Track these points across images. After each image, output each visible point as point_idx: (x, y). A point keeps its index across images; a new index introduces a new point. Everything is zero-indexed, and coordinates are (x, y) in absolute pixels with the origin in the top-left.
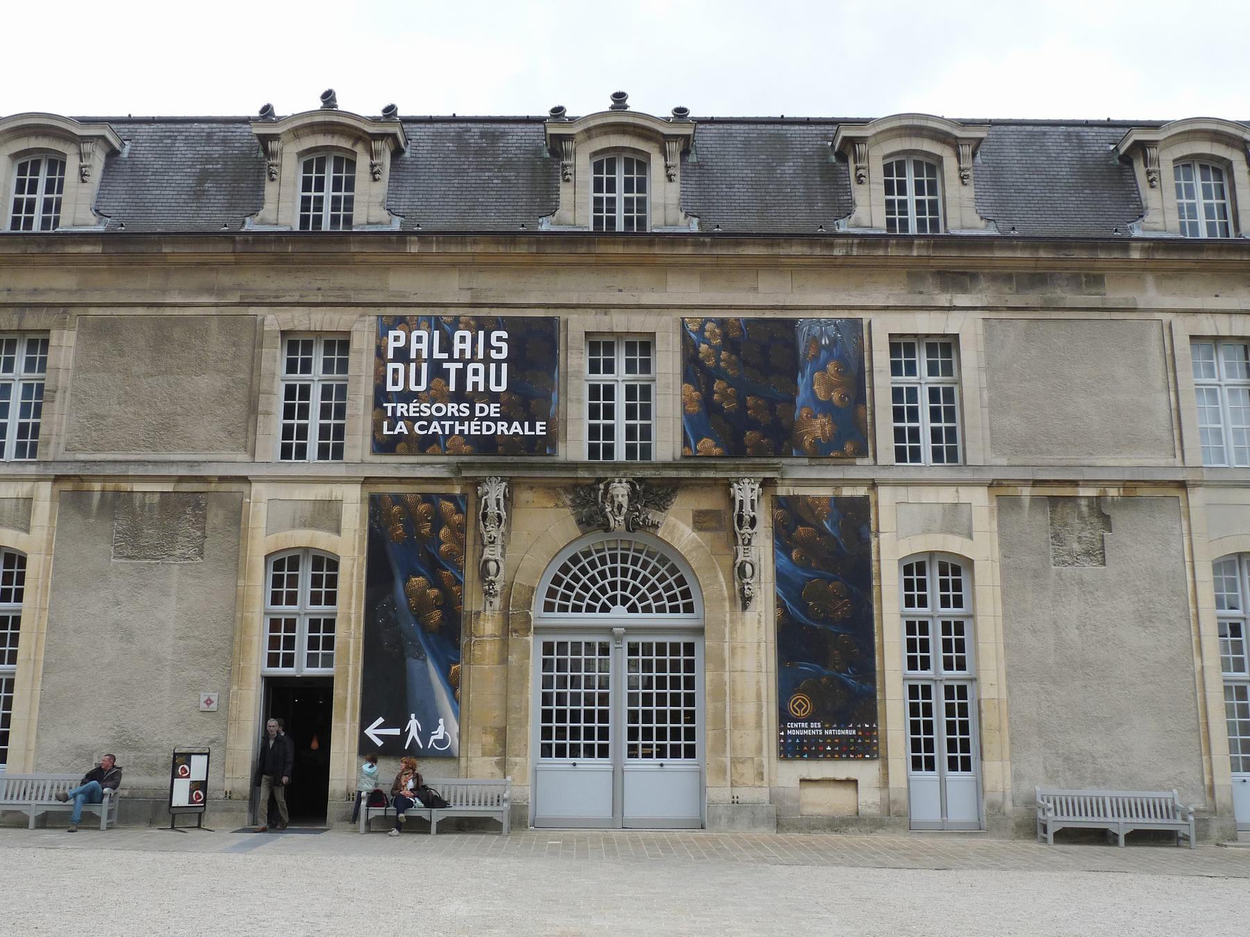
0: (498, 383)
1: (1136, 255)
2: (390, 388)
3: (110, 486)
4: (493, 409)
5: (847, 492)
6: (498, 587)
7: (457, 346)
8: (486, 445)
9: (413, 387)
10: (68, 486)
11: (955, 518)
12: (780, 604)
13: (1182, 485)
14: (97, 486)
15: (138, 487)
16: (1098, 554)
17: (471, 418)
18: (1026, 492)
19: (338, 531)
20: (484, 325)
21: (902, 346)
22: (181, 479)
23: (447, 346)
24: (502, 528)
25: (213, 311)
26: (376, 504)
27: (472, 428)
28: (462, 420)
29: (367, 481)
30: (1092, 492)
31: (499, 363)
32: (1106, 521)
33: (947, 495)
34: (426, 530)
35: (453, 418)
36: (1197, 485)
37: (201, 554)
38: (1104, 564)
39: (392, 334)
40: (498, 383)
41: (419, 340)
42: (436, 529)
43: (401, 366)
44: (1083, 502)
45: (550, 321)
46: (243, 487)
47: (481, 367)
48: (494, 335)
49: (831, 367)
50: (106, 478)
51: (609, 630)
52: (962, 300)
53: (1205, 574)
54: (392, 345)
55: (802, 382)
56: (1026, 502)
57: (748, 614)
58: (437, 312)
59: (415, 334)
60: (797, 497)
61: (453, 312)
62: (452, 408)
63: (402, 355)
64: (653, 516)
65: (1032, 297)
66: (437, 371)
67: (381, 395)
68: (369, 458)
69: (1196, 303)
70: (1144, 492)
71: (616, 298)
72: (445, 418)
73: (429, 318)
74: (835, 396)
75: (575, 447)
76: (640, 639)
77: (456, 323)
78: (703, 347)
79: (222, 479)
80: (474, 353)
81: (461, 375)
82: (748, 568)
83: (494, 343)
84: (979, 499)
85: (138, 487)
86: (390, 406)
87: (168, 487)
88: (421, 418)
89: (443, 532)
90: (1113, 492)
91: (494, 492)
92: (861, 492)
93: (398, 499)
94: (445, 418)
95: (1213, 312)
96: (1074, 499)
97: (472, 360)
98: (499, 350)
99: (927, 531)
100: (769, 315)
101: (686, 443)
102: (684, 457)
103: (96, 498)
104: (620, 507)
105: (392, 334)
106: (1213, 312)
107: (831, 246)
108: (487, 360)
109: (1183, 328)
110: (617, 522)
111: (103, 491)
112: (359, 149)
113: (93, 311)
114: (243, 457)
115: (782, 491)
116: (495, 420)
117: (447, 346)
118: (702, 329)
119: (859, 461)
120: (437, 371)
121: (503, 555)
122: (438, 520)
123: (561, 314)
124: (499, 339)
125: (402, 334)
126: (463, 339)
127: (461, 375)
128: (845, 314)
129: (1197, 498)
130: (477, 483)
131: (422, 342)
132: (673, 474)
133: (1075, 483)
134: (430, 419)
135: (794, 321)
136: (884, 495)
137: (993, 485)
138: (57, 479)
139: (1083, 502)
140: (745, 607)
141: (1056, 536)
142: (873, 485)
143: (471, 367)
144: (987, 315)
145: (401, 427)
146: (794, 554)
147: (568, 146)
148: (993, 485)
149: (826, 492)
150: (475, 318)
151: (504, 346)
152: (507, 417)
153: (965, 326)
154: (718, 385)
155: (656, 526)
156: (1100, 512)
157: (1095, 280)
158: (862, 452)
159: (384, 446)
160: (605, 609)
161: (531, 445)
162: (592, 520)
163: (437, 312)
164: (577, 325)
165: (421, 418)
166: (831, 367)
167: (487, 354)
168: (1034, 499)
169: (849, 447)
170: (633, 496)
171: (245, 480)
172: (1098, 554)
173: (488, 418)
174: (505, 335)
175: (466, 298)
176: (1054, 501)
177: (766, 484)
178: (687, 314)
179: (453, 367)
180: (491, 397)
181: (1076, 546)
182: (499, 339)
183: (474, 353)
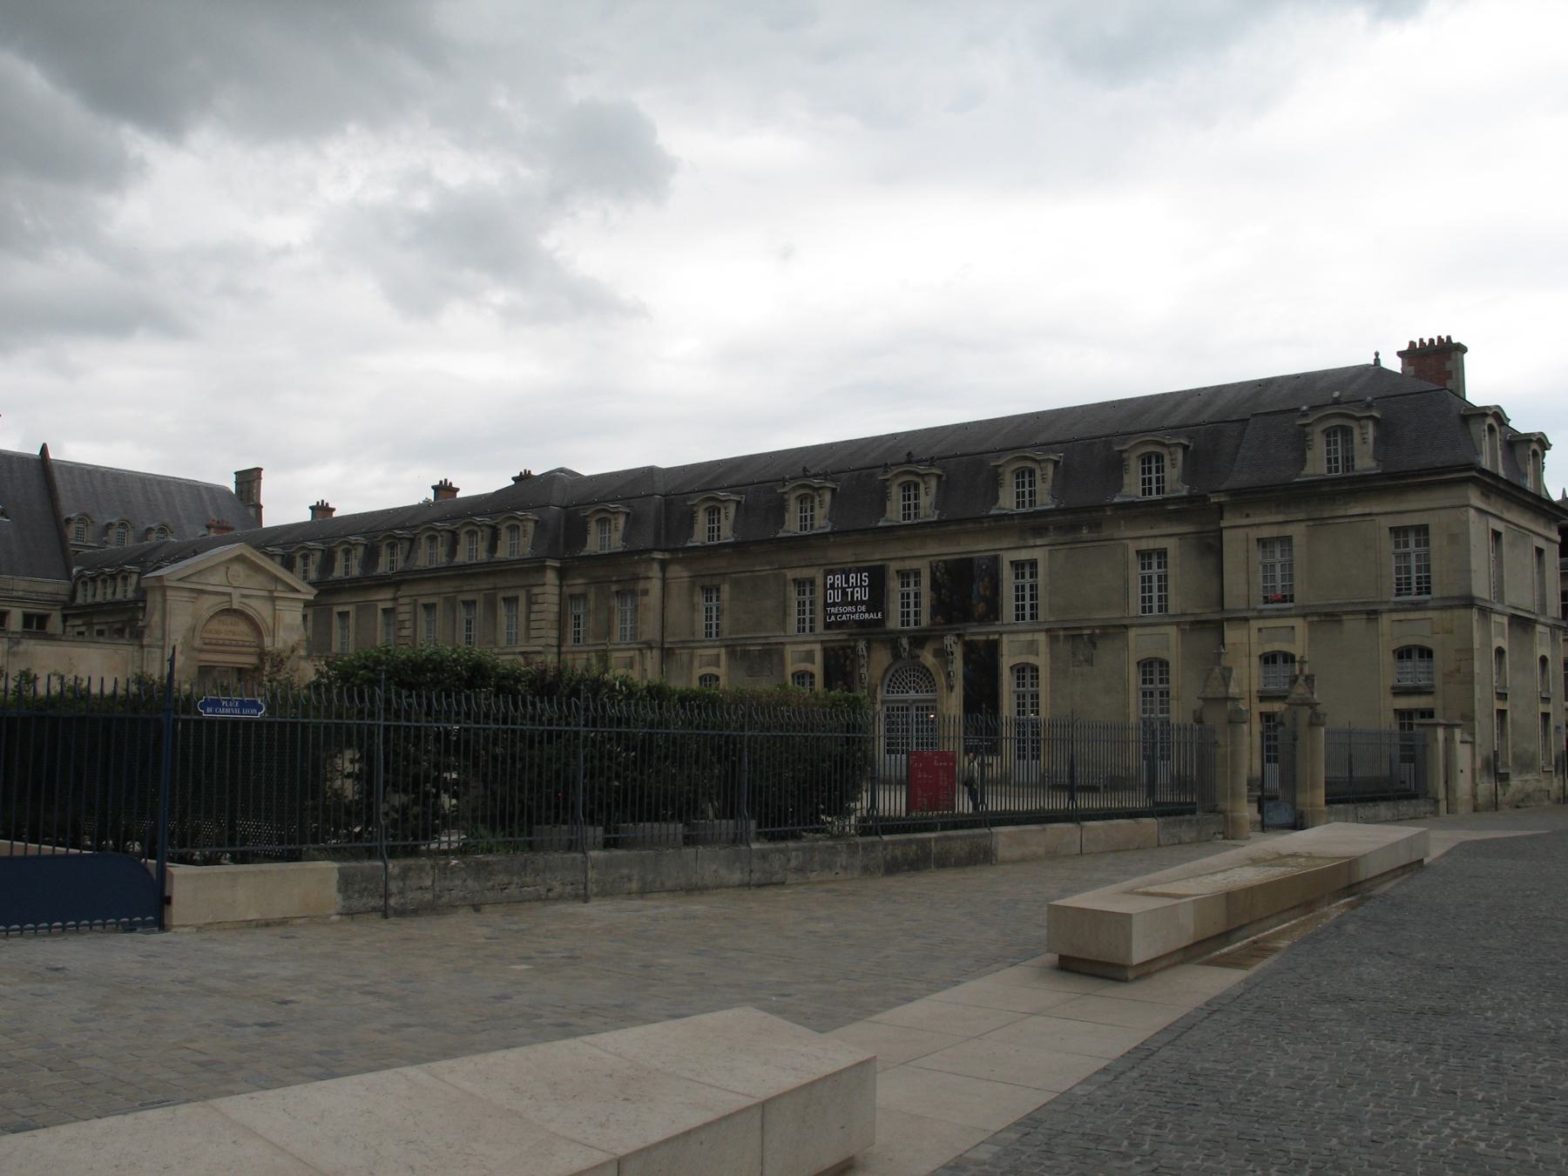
0: (865, 596)
1: (1109, 513)
2: (829, 601)
3: (743, 648)
4: (864, 608)
5: (991, 637)
6: (866, 685)
7: (851, 581)
8: (861, 623)
9: (836, 600)
10: (729, 649)
11: (1032, 647)
12: (964, 689)
13: (1126, 627)
14: (739, 649)
15: (751, 648)
16: (1089, 661)
17: (856, 612)
18: (1061, 633)
19: (814, 663)
20: (859, 570)
21: (1018, 565)
22: (764, 644)
23: (847, 581)
24: (866, 659)
25: (770, 572)
26: (826, 652)
27: (856, 617)
28: (853, 614)
29: (822, 642)
30: (1088, 632)
31: (865, 587)
32: (1094, 646)
33: (1029, 637)
34: (842, 661)
35: (850, 613)
36: (1132, 626)
37: (772, 674)
38: (1092, 665)
39: (829, 577)
40: (865, 596)
41: (838, 579)
42: (845, 661)
43: (832, 592)
44: (1085, 637)
45: (882, 567)
46: (781, 647)
47: (859, 589)
48: (863, 575)
49: (986, 579)
50: (741, 645)
51: (906, 701)
52: (1039, 542)
53: (1133, 668)
54: (829, 582)
55: (975, 587)
56: (1062, 638)
57: (953, 694)
58: (844, 566)
59: (836, 577)
60: (972, 641)
61: (850, 565)
62: (849, 609)
63: (832, 585)
64: (918, 652)
65: (1069, 538)
66: (845, 593)
67: (826, 605)
68: (824, 632)
69: (1139, 533)
70: (1111, 631)
71: (907, 554)
72: (847, 613)
73: (840, 569)
74: (987, 593)
75: (894, 623)
76: (920, 705)
77: (850, 571)
78: (938, 574)
79: (776, 644)
80: (857, 583)
81: (852, 593)
82: (952, 673)
83: (863, 578)
84: (1042, 638)
85: (751, 648)
86: (829, 609)
87: (760, 648)
88: (839, 614)
89: (848, 662)
90: (1097, 631)
91: (862, 645)
92: (996, 637)
93: (833, 649)
94: (847, 613)
95: (1155, 537)
96: (1082, 635)
97: (857, 586)
98: (865, 581)
99: (1021, 654)
100: (964, 556)
101: (931, 619)
102: (932, 625)
103: (739, 653)
104: (905, 649)
105: (829, 577)
106: (1155, 537)
107: (983, 523)
108: (861, 586)
109: (1133, 547)
110: (905, 655)
111: (741, 650)
112: (815, 494)
113: (733, 575)
114: (783, 634)
115: (967, 638)
116: (864, 613)
117: (847, 581)
118: (937, 567)
119: (996, 623)
120: (845, 593)
121: (868, 671)
122: (846, 657)
123: (887, 563)
124: (865, 576)
125: (832, 577)
126: (853, 578)
127: (852, 593)
128: (993, 553)
129: (1132, 633)
130: (856, 641)
131: (839, 580)
132: (927, 633)
133: (1080, 628)
134: (843, 613)
135: (971, 560)
136: (1005, 637)
137: (1047, 631)
138: (726, 646)
139: (1085, 637)
140: (951, 691)
141: (1074, 654)
142: (1001, 634)
143: (856, 589)
144: (1049, 548)
145: (833, 618)
146: (970, 667)
147: (888, 483)
148: (1047, 631)
149: (983, 638)
150: (857, 568)
151: (867, 579)
152: (868, 611)
153: (1039, 554)
154: (943, 591)
155: (919, 657)
156: (1092, 641)
157: (1095, 526)
158: (997, 619)
159: (828, 626)
160: (907, 692)
161: (880, 623)
162: (896, 656)
163: (844, 566)
164: (893, 567)
165: (839, 614)
166: (986, 579)
167: (861, 583)
168: (1065, 636)
169: (992, 617)
170: (910, 644)
171: (782, 643)
172: (1089, 661)
173: (862, 612)
174: (867, 574)
175: (853, 558)
176: (1074, 636)
177: (959, 636)
178: (931, 559)
179: (849, 590)
180: (862, 602)
181: (1081, 658)
182: (865, 576)
183: (857, 583)
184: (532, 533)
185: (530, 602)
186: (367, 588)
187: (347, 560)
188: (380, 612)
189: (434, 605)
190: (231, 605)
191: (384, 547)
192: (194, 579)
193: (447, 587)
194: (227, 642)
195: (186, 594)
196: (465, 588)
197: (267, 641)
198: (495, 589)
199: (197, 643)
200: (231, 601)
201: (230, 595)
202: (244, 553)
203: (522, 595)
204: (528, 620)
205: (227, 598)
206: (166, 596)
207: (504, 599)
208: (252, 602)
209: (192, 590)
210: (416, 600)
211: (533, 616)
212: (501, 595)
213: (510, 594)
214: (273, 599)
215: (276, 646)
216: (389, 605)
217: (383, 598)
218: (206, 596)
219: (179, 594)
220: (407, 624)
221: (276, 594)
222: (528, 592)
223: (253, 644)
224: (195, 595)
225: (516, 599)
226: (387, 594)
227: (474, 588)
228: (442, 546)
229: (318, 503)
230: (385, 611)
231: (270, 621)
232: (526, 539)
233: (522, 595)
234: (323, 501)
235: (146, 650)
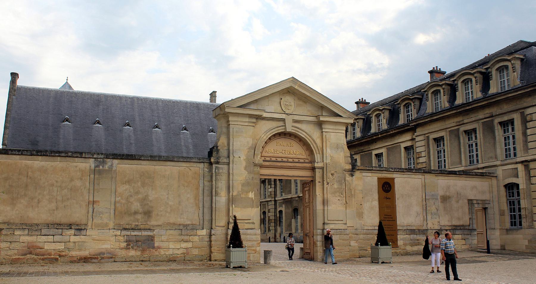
184: (520, 69)
185: (525, 121)
186: (393, 136)
187: (379, 121)
188: (403, 150)
189: (442, 138)
190: (286, 129)
191: (402, 108)
192: (252, 107)
193: (451, 123)
194: (285, 160)
195: (247, 120)
196: (465, 121)
197: (318, 157)
198: (492, 116)
199: (258, 160)
200: (285, 126)
201: (283, 120)
202: (293, 86)
203: (517, 117)
204: (525, 134)
205: (281, 123)
206: (228, 121)
207: (500, 123)
208: (303, 126)
209: (251, 116)
210: (428, 137)
211: (529, 132)
212: (497, 121)
213: (505, 118)
214: (320, 124)
215: (325, 161)
216: (409, 144)
217: (404, 140)
218: (263, 122)
219: (240, 119)
220: (423, 154)
221: (322, 119)
222: (522, 114)
223: (307, 161)
224: (254, 120)
225: (512, 122)
226: (407, 137)
227: (473, 119)
228: (444, 95)
229: (360, 100)
230: (406, 148)
231: (318, 142)
232: (515, 73)
233: (517, 117)
234: (362, 99)
235: (214, 166)
